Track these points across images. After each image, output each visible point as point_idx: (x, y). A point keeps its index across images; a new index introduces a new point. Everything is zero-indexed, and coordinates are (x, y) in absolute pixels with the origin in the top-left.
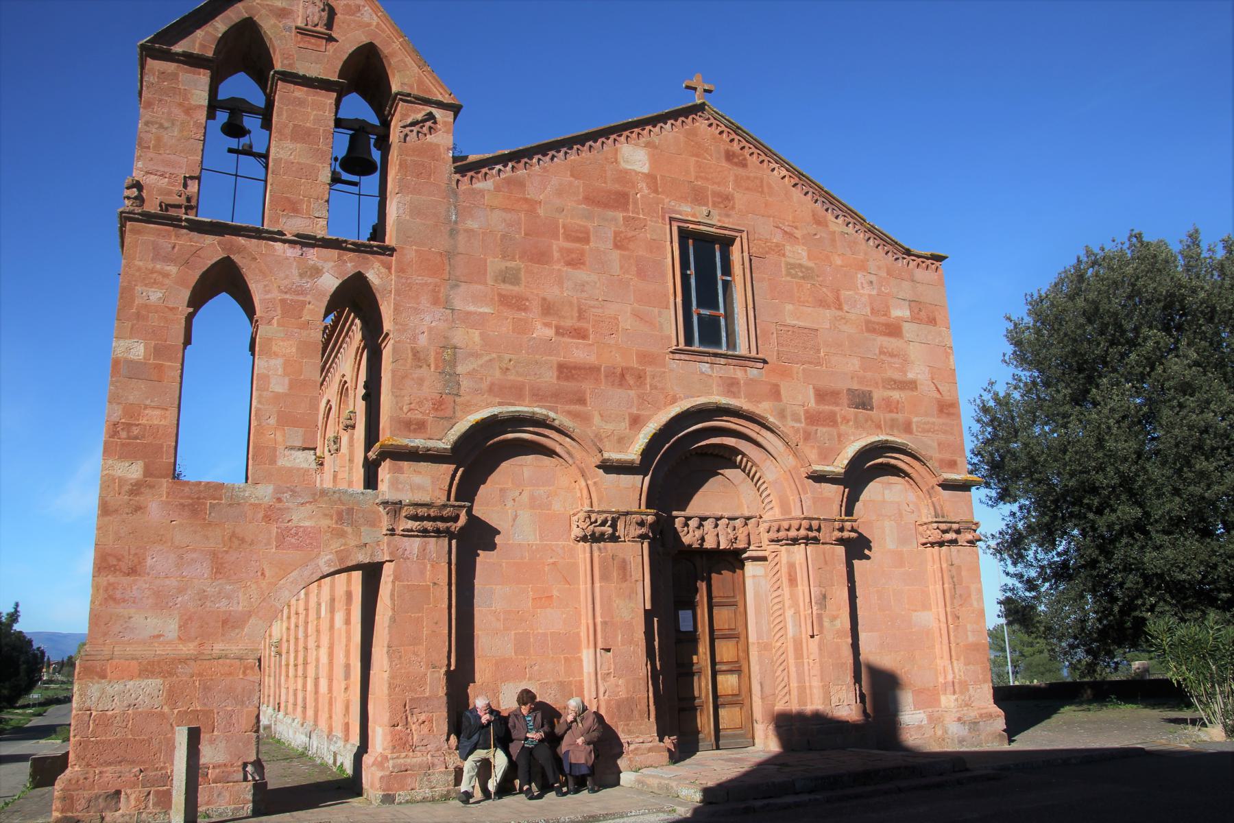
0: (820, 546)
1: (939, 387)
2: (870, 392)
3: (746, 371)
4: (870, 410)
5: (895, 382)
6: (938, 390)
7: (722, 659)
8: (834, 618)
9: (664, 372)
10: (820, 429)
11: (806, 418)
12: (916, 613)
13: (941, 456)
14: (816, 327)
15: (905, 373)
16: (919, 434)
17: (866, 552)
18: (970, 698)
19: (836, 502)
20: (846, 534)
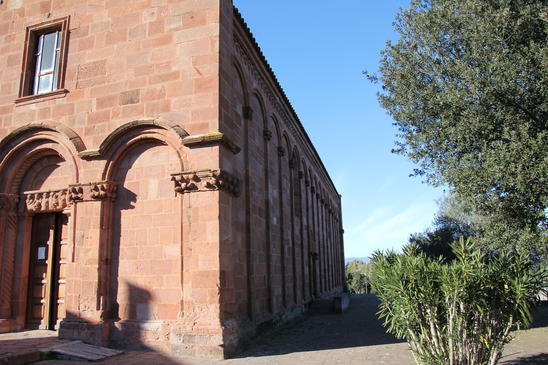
0: (85, 202)
1: (201, 70)
2: (139, 90)
3: (55, 101)
4: (136, 103)
5: (160, 77)
6: (198, 72)
7: (62, 276)
8: (87, 251)
9: (12, 115)
10: (96, 125)
11: (89, 120)
12: (167, 246)
13: (193, 123)
14: (104, 58)
15: (170, 68)
16: (175, 110)
17: (132, 203)
18: (195, 315)
19: (100, 172)
20: (96, 194)
